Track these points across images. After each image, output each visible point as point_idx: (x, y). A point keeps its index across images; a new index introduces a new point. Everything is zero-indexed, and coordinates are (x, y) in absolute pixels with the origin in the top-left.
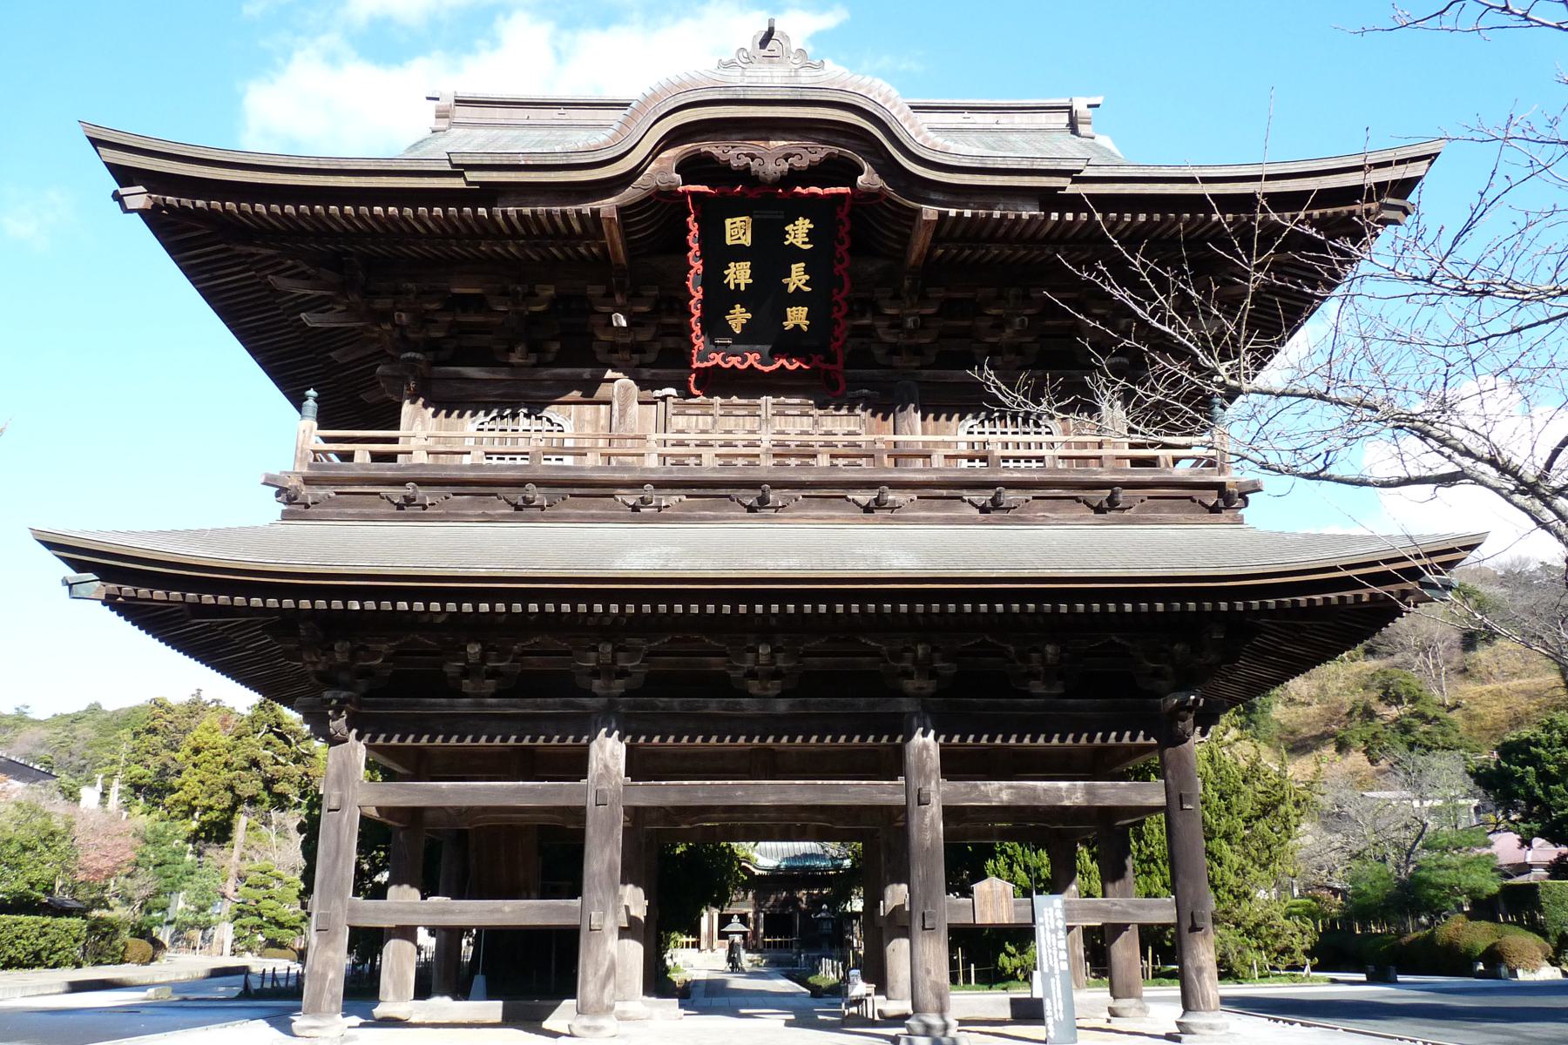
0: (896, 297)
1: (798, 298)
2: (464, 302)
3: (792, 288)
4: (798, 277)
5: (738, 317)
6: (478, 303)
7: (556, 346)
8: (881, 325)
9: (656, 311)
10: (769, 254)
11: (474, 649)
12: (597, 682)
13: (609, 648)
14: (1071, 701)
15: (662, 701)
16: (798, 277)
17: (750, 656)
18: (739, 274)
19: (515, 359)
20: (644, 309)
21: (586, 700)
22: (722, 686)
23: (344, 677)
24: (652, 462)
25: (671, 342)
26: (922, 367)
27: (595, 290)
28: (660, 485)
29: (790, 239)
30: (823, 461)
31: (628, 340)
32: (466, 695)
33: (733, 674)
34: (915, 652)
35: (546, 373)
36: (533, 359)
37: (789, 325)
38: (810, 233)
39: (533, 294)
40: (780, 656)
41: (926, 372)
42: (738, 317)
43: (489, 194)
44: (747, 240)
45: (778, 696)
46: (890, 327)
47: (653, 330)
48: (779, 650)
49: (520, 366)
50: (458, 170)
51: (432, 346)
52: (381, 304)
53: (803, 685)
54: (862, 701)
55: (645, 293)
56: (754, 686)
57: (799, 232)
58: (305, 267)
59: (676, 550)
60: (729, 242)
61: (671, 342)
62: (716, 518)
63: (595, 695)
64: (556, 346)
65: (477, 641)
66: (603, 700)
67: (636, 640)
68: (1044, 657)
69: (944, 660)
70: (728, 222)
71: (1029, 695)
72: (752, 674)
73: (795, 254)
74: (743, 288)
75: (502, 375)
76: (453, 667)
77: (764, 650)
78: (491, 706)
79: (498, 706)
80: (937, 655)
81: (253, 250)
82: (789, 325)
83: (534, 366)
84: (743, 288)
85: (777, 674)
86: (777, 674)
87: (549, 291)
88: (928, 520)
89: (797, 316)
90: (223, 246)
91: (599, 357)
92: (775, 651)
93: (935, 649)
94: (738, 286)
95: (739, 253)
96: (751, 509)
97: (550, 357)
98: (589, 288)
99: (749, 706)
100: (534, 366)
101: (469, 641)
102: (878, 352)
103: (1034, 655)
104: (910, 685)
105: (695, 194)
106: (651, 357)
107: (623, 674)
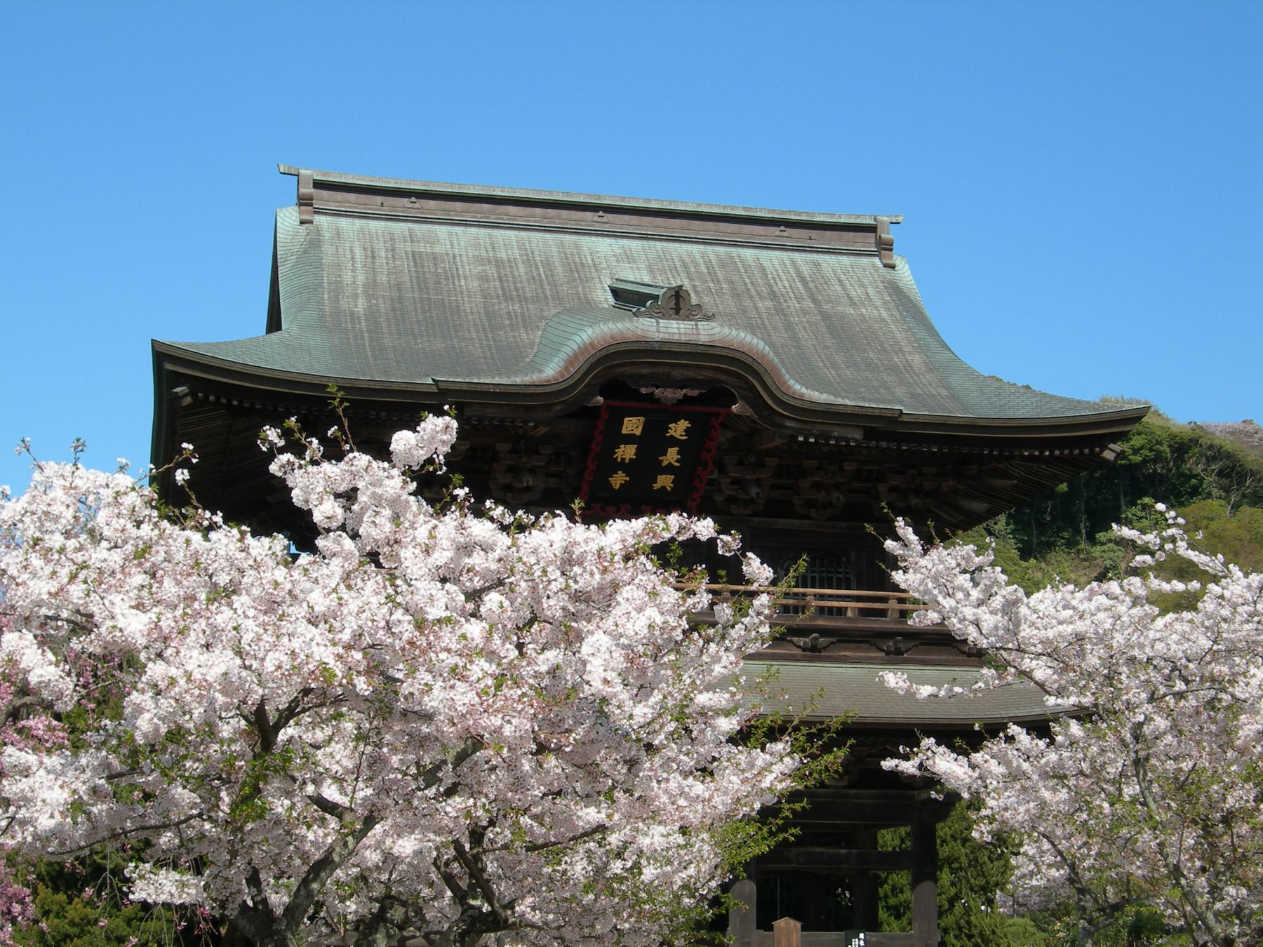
0: (740, 463)
1: (669, 469)
3: (665, 463)
4: (672, 456)
5: (618, 479)
8: (725, 481)
10: (653, 441)
14: (853, 791)
16: (672, 456)
18: (627, 452)
25: (552, 482)
26: (754, 514)
27: (503, 447)
29: (671, 432)
37: (656, 486)
38: (687, 430)
41: (756, 519)
42: (618, 479)
44: (638, 432)
46: (732, 483)
57: (679, 429)
60: (624, 431)
61: (552, 482)
70: (626, 419)
73: (673, 442)
82: (656, 486)
94: (623, 459)
95: (630, 439)
102: (719, 498)
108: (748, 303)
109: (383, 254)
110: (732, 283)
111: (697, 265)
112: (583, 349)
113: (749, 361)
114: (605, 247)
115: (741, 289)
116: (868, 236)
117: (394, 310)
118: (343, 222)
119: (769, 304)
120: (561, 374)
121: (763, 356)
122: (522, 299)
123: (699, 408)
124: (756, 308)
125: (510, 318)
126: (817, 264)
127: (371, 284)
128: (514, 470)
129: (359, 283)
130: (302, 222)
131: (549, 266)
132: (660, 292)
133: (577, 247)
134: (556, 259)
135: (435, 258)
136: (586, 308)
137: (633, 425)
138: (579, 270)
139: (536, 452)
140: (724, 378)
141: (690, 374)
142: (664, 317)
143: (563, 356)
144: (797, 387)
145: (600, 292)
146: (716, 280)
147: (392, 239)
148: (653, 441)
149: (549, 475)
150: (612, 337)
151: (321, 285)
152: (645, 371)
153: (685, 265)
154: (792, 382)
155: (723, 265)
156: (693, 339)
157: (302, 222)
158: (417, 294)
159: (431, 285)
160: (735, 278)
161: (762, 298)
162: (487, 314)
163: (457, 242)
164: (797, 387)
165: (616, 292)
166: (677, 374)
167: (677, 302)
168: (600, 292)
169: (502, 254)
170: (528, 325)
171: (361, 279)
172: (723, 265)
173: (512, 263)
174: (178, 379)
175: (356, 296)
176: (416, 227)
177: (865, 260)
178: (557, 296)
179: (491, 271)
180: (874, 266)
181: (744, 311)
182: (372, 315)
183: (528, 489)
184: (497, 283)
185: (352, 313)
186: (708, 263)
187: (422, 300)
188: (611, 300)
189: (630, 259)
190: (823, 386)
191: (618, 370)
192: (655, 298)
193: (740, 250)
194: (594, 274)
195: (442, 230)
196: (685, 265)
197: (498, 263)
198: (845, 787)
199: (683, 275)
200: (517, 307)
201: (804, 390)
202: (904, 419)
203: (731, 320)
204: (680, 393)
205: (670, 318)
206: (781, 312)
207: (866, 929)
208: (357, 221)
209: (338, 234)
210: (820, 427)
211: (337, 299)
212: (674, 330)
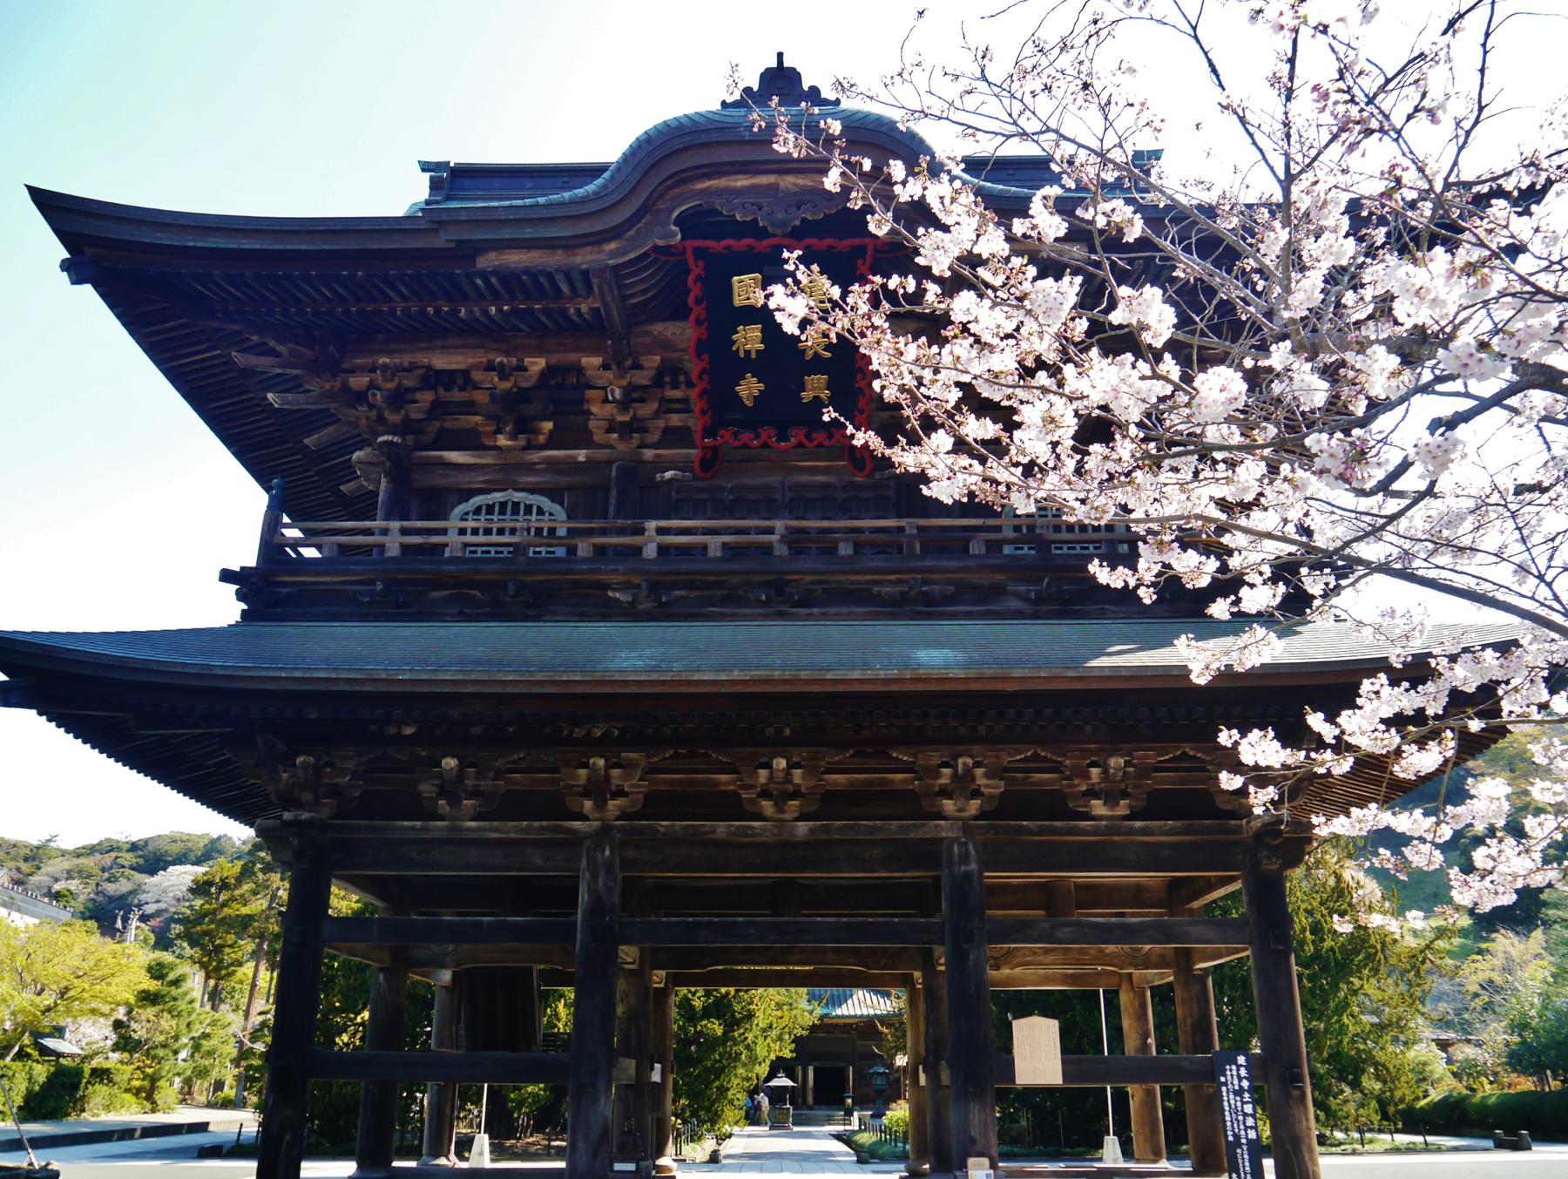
5: (749, 388)
6: (463, 379)
7: (548, 426)
9: (658, 382)
11: (450, 763)
12: (588, 804)
13: (601, 762)
14: (1138, 824)
17: (763, 773)
19: (502, 441)
20: (646, 382)
21: (577, 824)
22: (731, 807)
23: (307, 797)
25: (676, 420)
27: (591, 361)
31: (626, 418)
32: (442, 818)
34: (955, 767)
35: (535, 456)
36: (522, 442)
40: (798, 773)
42: (749, 388)
43: (467, 251)
45: (796, 819)
47: (655, 405)
48: (798, 766)
49: (509, 449)
51: (406, 427)
55: (646, 365)
58: (272, 343)
60: (737, 302)
63: (586, 819)
64: (548, 426)
65: (453, 756)
66: (597, 824)
67: (632, 755)
68: (1105, 772)
69: (987, 776)
71: (1087, 816)
72: (765, 794)
74: (753, 356)
75: (488, 459)
76: (427, 789)
78: (470, 829)
79: (477, 830)
80: (979, 771)
81: (215, 324)
83: (524, 449)
84: (753, 356)
87: (537, 364)
88: (969, 616)
90: (184, 321)
91: (595, 438)
92: (792, 766)
93: (978, 765)
96: (765, 604)
97: (542, 438)
98: (584, 360)
100: (524, 449)
101: (445, 756)
103: (1095, 771)
104: (949, 805)
105: (699, 253)
106: (654, 437)
107: (619, 793)
191: (700, 186)
198: (1125, 818)
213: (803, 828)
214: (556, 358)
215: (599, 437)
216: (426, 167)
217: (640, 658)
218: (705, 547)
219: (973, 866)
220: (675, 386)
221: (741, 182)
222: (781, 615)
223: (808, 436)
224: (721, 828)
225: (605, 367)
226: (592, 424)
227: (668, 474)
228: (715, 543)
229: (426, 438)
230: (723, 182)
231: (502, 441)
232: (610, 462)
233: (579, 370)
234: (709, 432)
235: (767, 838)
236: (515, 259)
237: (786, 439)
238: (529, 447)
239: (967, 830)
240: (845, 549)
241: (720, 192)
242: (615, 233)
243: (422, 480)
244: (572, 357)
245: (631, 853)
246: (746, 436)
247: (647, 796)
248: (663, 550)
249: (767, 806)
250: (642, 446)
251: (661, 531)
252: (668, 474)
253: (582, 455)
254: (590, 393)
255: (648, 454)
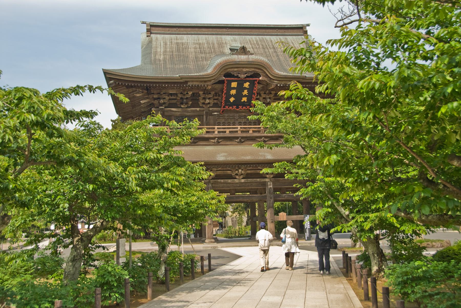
0: (265, 93)
1: (245, 96)
2: (171, 94)
4: (245, 92)
5: (232, 99)
7: (191, 103)
10: (240, 88)
15: (219, 180)
16: (245, 92)
18: (233, 92)
19: (182, 106)
22: (231, 177)
24: (216, 133)
25: (215, 101)
27: (201, 93)
28: (219, 138)
30: (251, 132)
33: (233, 174)
37: (242, 101)
38: (249, 85)
39: (187, 93)
42: (232, 99)
43: (186, 82)
44: (236, 86)
50: (181, 79)
52: (155, 96)
53: (247, 176)
54: (258, 179)
56: (237, 177)
57: (247, 85)
59: (226, 154)
61: (215, 101)
62: (230, 144)
72: (237, 174)
73: (246, 88)
75: (180, 110)
77: (240, 170)
82: (242, 101)
85: (242, 174)
86: (242, 174)
87: (190, 93)
89: (244, 99)
95: (234, 88)
97: (189, 105)
99: (236, 181)
105: (227, 80)
106: (211, 105)
108: (266, 50)
109: (169, 43)
110: (263, 45)
111: (253, 41)
112: (218, 65)
113: (263, 65)
114: (228, 38)
115: (265, 47)
116: (301, 30)
117: (171, 58)
118: (158, 36)
119: (273, 50)
120: (212, 71)
121: (267, 64)
122: (205, 53)
123: (251, 79)
124: (269, 51)
125: (202, 58)
126: (286, 39)
127: (165, 52)
128: (204, 99)
129: (162, 51)
130: (147, 36)
131: (213, 44)
132: (239, 48)
133: (221, 38)
134: (215, 42)
135: (183, 44)
136: (223, 54)
137: (234, 85)
138: (221, 45)
139: (210, 93)
140: (257, 70)
141: (248, 70)
142: (240, 55)
143: (213, 67)
144: (277, 71)
145: (226, 50)
146: (258, 45)
147: (171, 39)
148: (240, 88)
149: (214, 100)
150: (226, 61)
151: (151, 53)
152: (236, 70)
153: (250, 41)
154: (275, 70)
155: (261, 41)
156: (248, 60)
157: (147, 36)
158: (177, 53)
159: (181, 50)
160: (264, 44)
161: (270, 48)
162: (196, 57)
163: (188, 39)
164: (277, 71)
165: (230, 49)
166: (245, 70)
167: (244, 50)
168: (226, 50)
169: (201, 42)
170: (206, 59)
171: (162, 50)
172: (261, 41)
173: (203, 44)
174: (111, 79)
175: (161, 55)
176: (178, 36)
177: (300, 37)
178: (215, 52)
179: (198, 46)
180: (302, 38)
181: (266, 52)
182: (165, 60)
183: (209, 103)
184: (199, 49)
185: (159, 59)
186: (257, 41)
187: (178, 55)
188: (230, 52)
189: (235, 41)
190: (285, 70)
191: (228, 70)
192: (237, 50)
193: (265, 36)
194: (225, 45)
195: (185, 37)
196: (250, 41)
197: (200, 44)
199: (249, 44)
200: (204, 55)
201: (279, 72)
202: (307, 78)
203: (262, 55)
204: (245, 76)
205: (242, 55)
206: (275, 52)
207: (309, 214)
208: (162, 35)
209: (157, 39)
210: (284, 82)
211: (156, 56)
212: (243, 58)
213: (243, 181)
214: (194, 91)
215: (201, 105)
216: (143, 23)
217: (222, 156)
218: (225, 132)
219: (271, 186)
220: (216, 96)
221: (236, 70)
222: (240, 145)
223: (242, 107)
224: (230, 181)
225: (204, 93)
226: (199, 102)
227: (215, 113)
228: (228, 131)
229: (166, 105)
230: (232, 70)
231: (182, 106)
232: (203, 111)
233: (199, 94)
234: (224, 107)
235: (237, 182)
236: (195, 83)
237: (239, 108)
238: (188, 107)
239: (271, 180)
240: (251, 132)
241: (232, 71)
242: (214, 79)
243: (166, 114)
244: (197, 91)
245: (214, 185)
246: (231, 108)
247: (216, 176)
248: (219, 132)
249: (237, 177)
250: (210, 107)
251: (218, 128)
252: (215, 113)
253: (198, 109)
254: (200, 98)
255: (211, 109)
